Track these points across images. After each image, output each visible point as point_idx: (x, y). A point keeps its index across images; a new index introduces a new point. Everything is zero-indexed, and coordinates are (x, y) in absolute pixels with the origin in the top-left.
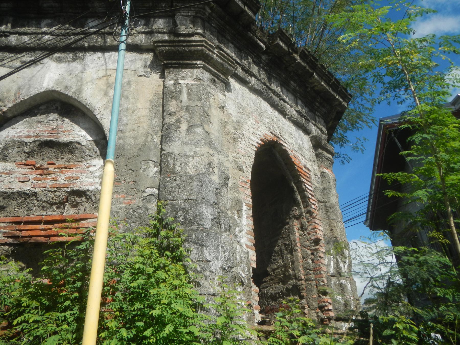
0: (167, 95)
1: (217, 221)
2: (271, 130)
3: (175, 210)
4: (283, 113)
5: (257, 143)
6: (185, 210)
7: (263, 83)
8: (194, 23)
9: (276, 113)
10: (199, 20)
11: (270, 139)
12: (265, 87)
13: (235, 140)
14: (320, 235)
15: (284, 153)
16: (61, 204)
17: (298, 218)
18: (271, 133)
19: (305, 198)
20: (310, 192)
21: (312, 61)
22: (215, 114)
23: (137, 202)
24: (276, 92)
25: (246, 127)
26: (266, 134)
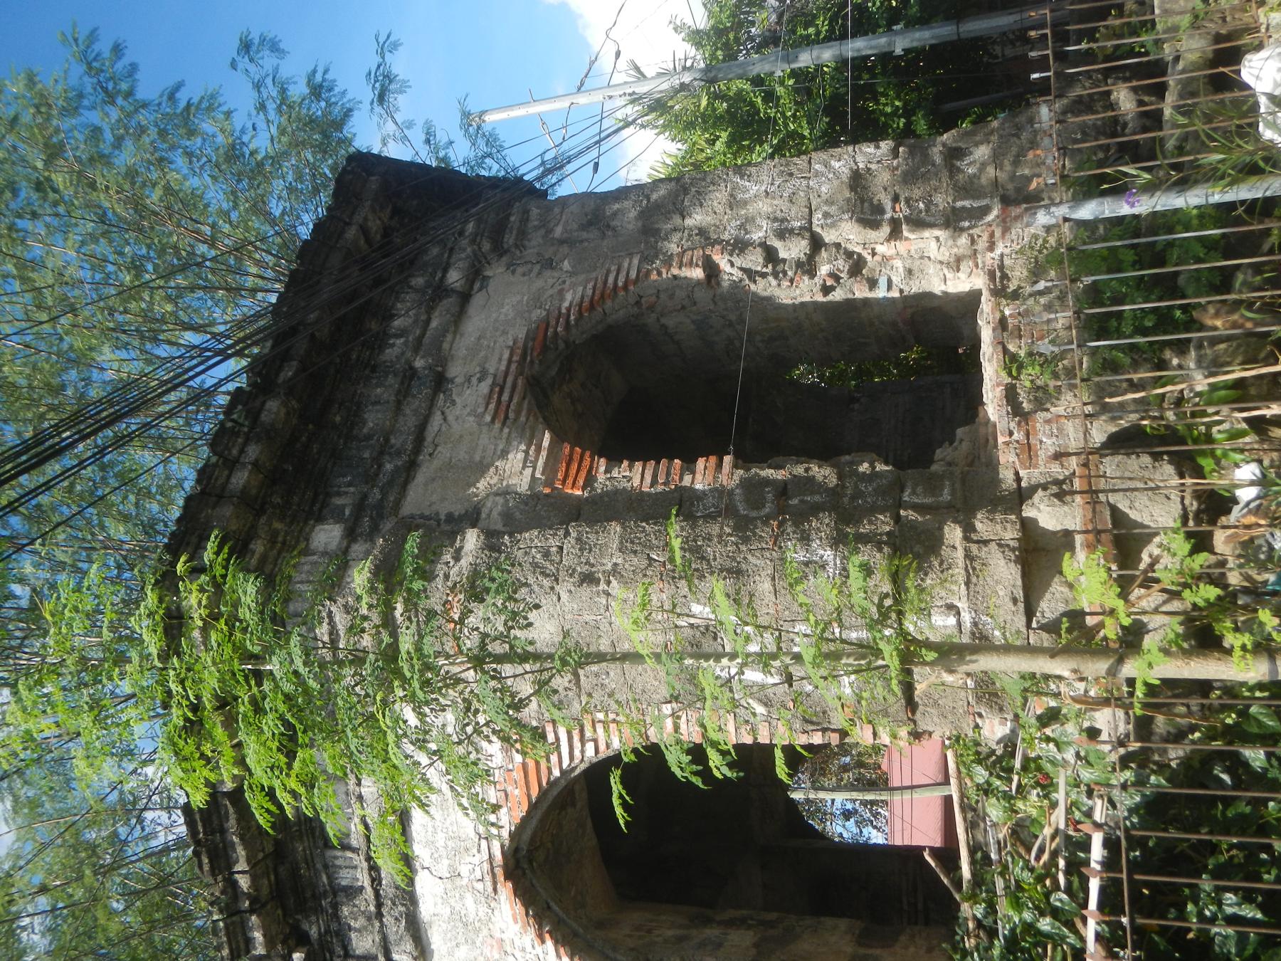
2: (490, 889)
5: (559, 956)
7: (381, 922)
9: (419, 850)
11: (519, 908)
12: (385, 911)
18: (495, 890)
20: (577, 745)
21: (204, 826)
24: (370, 875)
26: (516, 921)
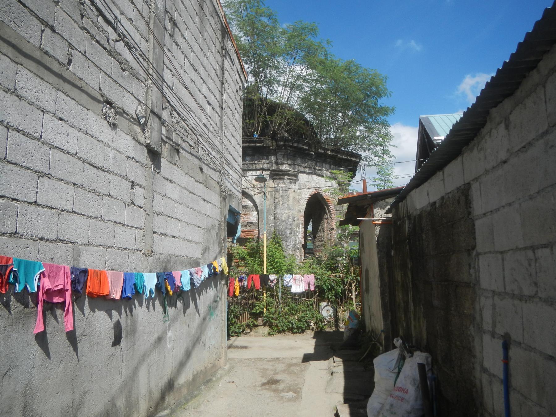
0: (276, 190)
1: (291, 234)
3: (279, 231)
4: (322, 176)
6: (282, 231)
8: (284, 157)
10: (286, 156)
13: (299, 201)
14: (334, 226)
15: (321, 196)
16: (246, 226)
17: (327, 219)
19: (329, 212)
22: (292, 195)
23: (268, 228)
25: (303, 193)
